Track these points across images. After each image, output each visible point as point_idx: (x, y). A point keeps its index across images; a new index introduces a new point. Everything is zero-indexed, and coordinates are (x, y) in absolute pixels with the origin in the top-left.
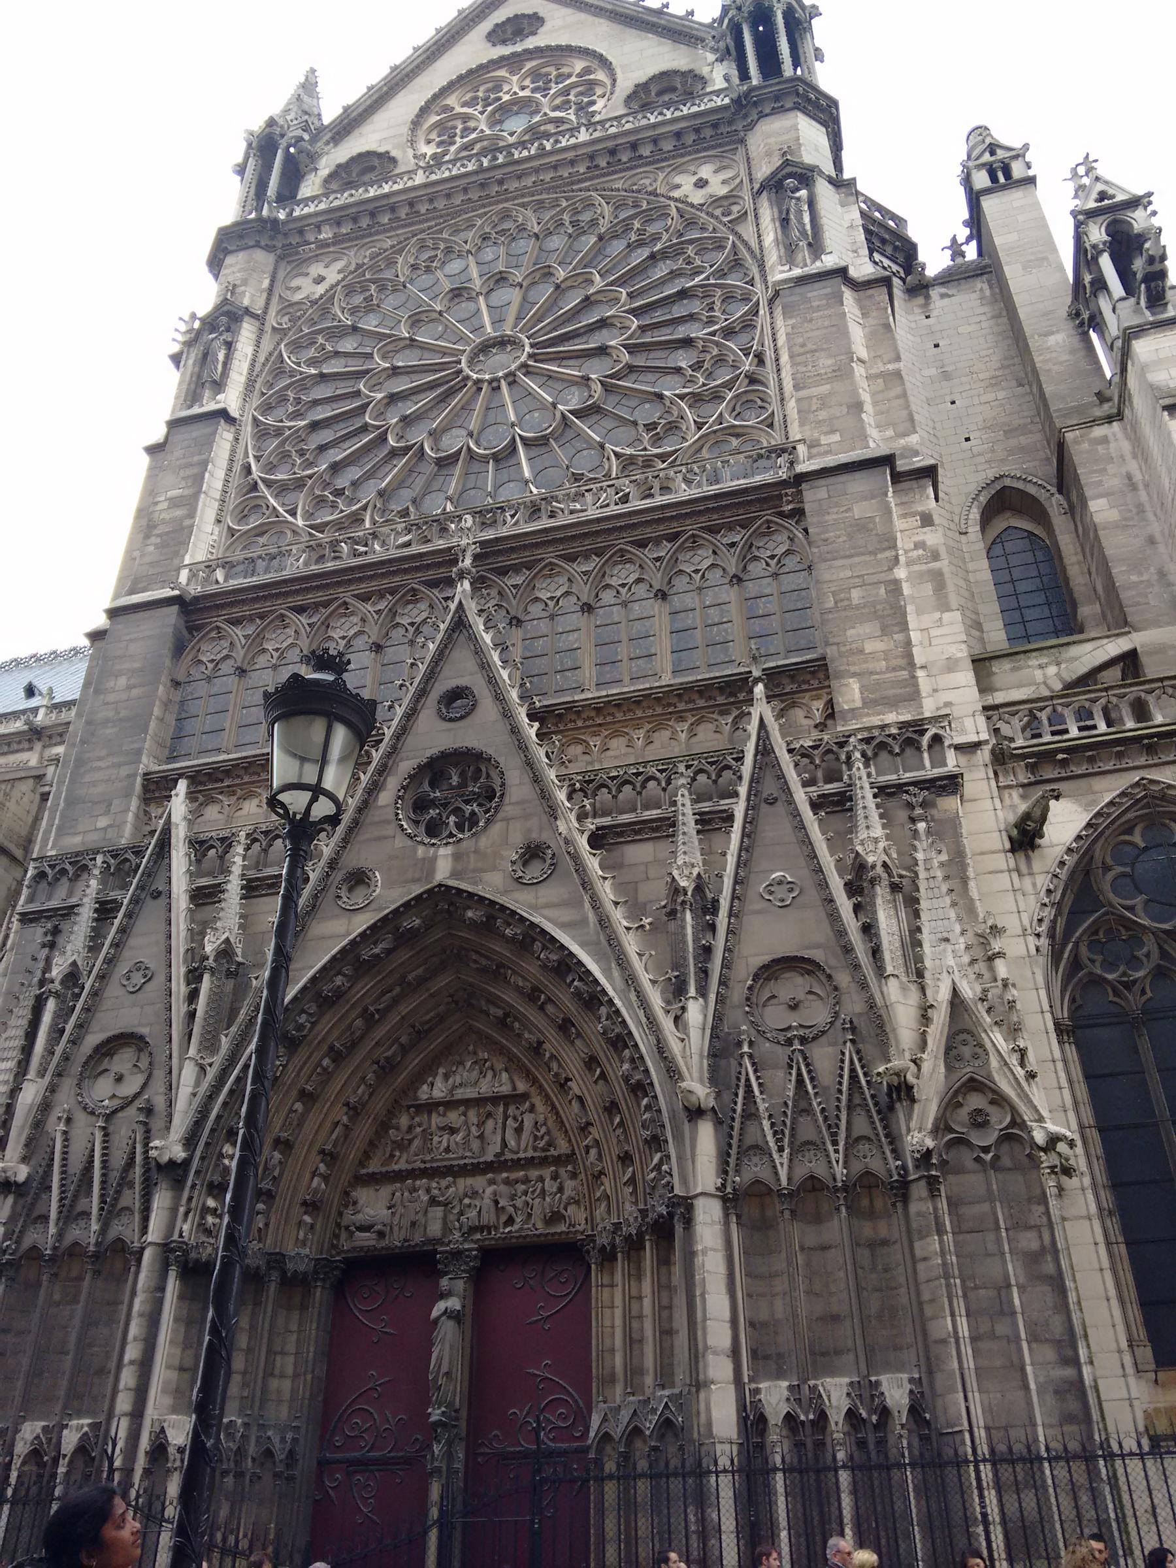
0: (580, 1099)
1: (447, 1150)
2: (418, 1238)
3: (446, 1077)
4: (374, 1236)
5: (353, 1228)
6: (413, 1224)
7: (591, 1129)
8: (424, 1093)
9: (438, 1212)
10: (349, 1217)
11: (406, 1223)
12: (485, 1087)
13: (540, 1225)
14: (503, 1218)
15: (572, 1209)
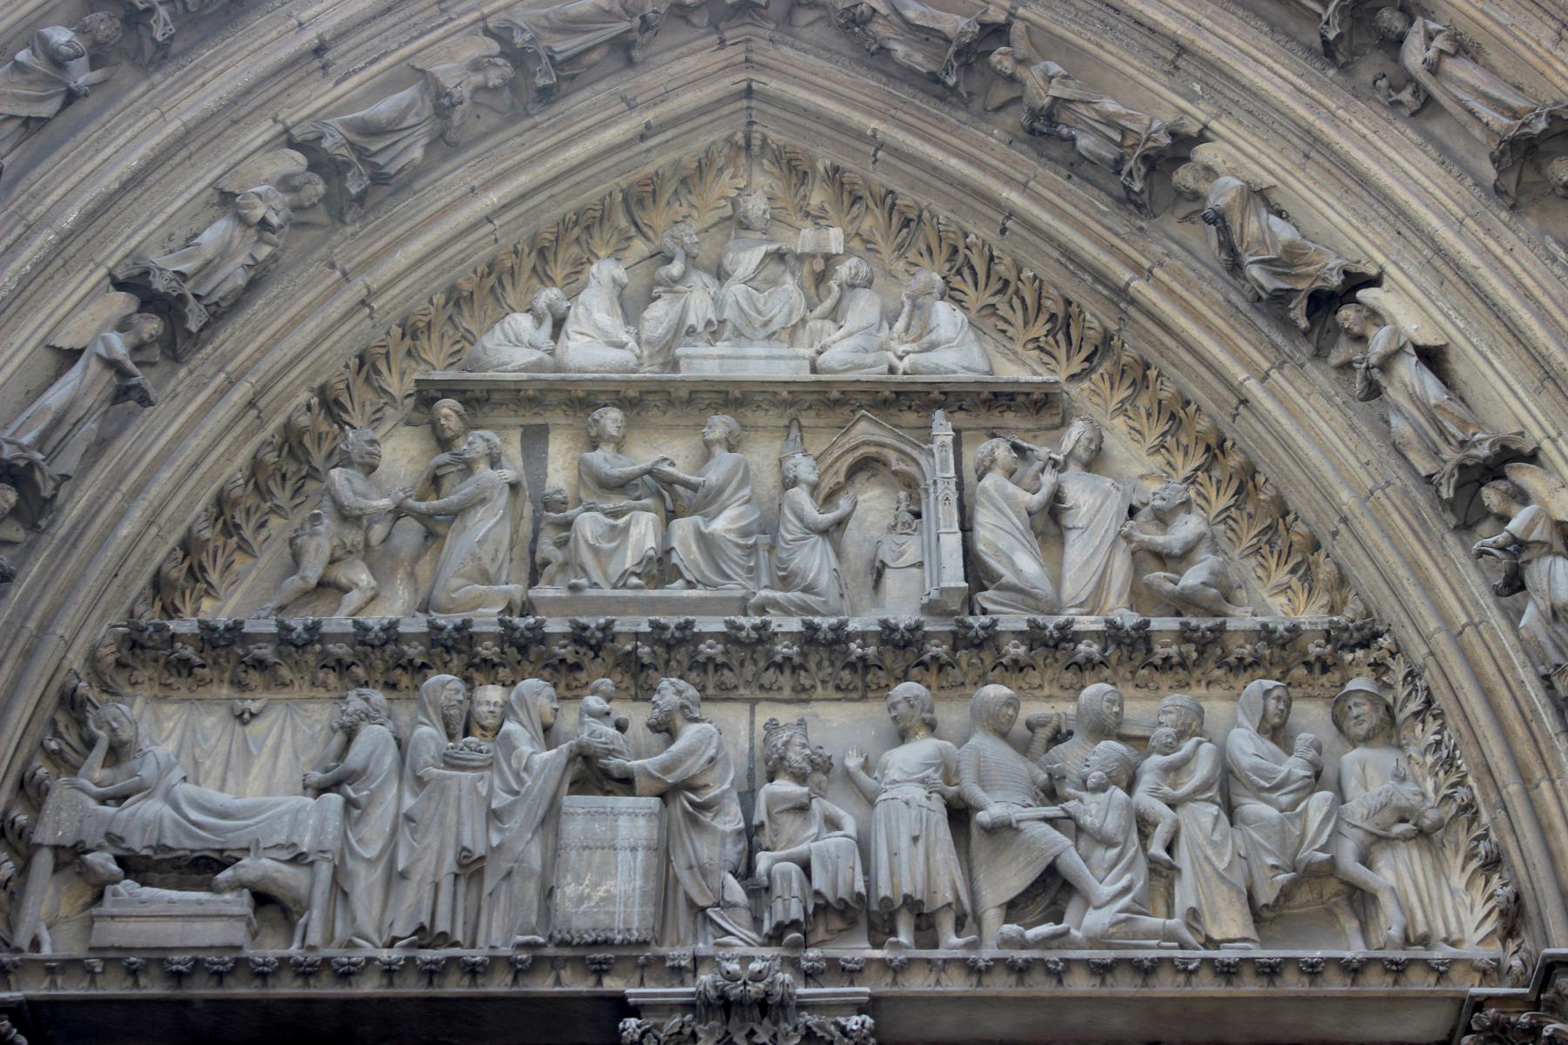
0: (1432, 358)
1: (660, 568)
2: (498, 934)
3: (631, 306)
4: (240, 903)
5: (103, 861)
6: (470, 868)
7: (1526, 476)
8: (512, 346)
9: (632, 819)
10: (71, 811)
11: (429, 859)
12: (851, 345)
13: (1230, 923)
14: (1006, 879)
15: (1396, 873)
